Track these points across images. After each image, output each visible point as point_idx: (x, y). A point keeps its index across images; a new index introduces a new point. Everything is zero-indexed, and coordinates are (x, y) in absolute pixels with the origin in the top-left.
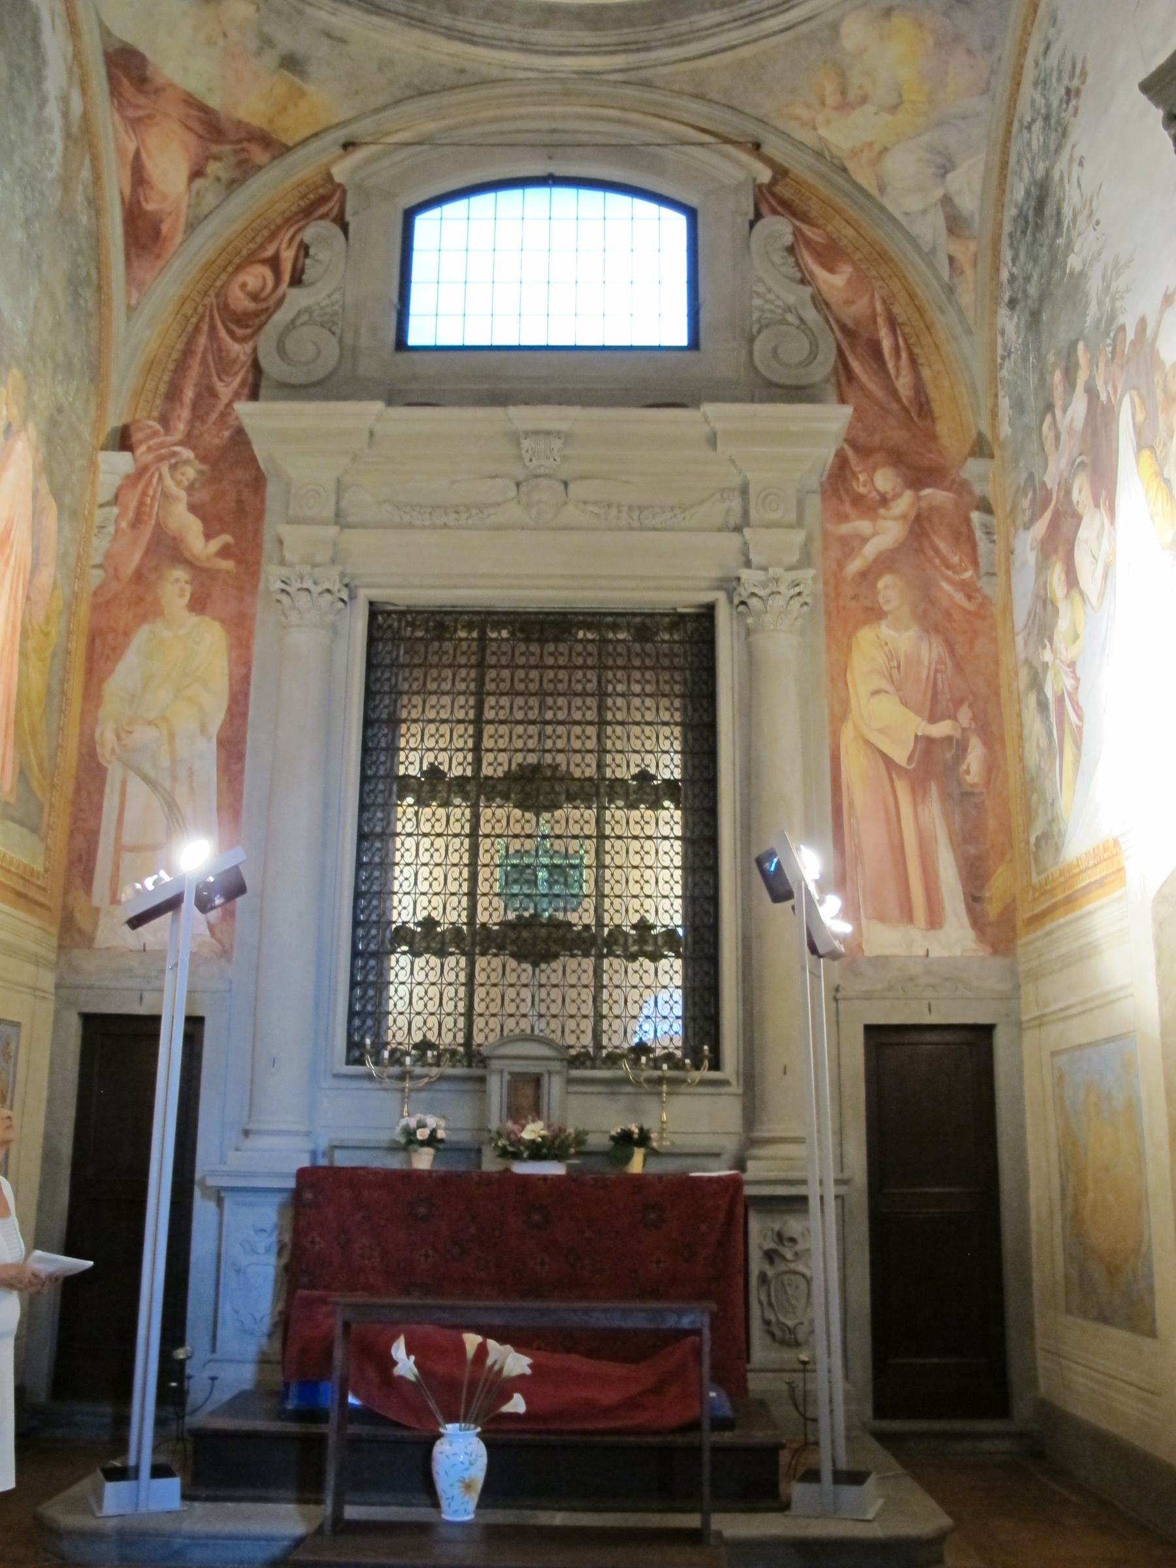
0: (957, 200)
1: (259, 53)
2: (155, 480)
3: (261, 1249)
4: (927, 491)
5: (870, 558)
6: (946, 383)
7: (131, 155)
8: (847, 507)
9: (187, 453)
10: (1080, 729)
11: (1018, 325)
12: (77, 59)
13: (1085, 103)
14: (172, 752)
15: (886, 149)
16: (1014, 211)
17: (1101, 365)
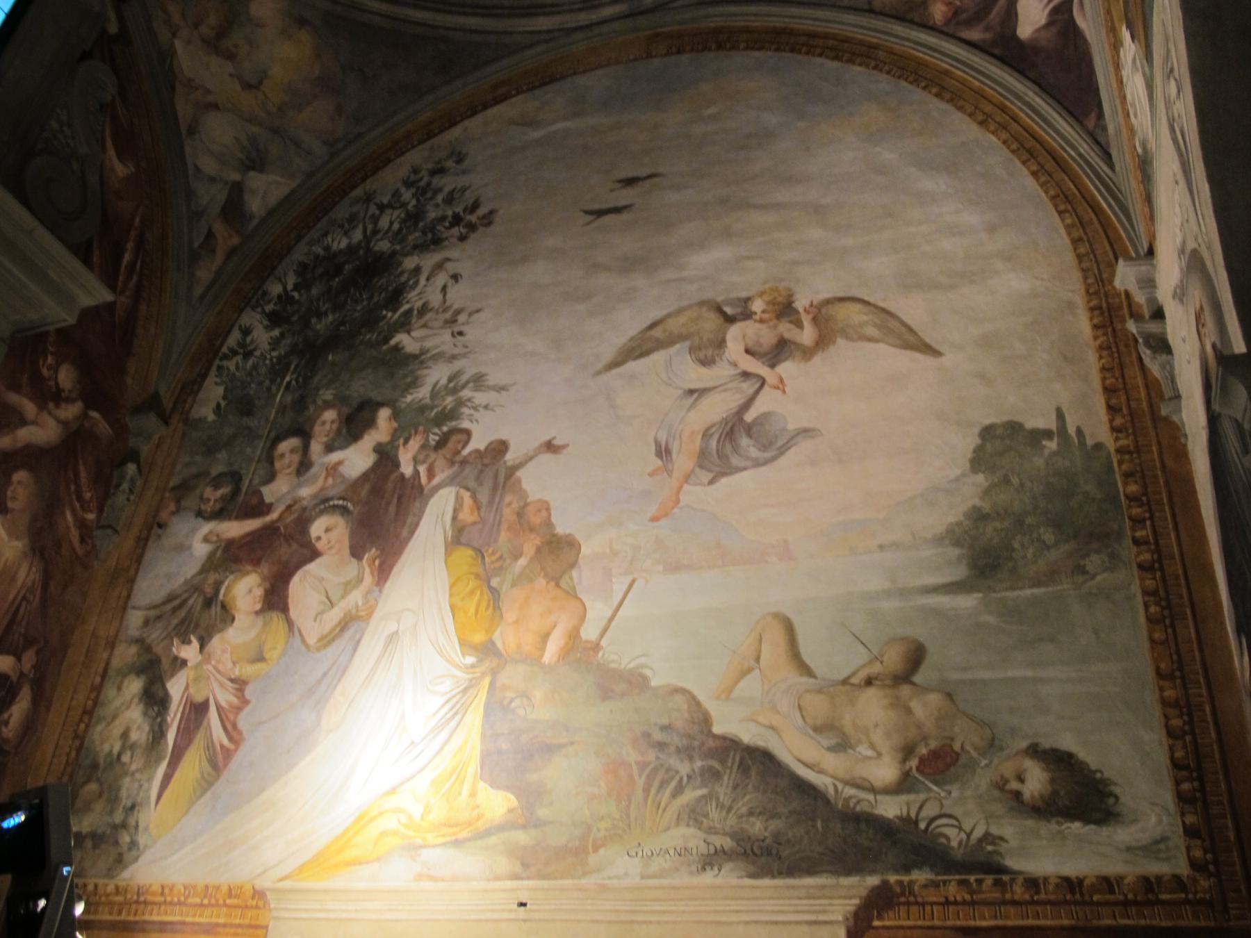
0: (247, 197)
4: (94, 414)
5: (20, 444)
13: (480, 242)
15: (215, 106)
16: (319, 250)
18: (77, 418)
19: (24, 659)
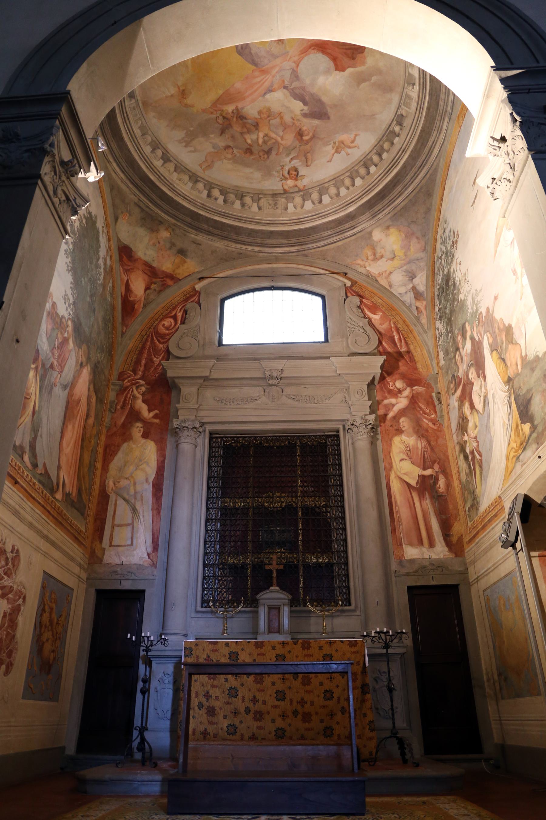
0: (418, 288)
1: (170, 248)
2: (130, 392)
3: (166, 682)
5: (396, 412)
6: (419, 350)
7: (125, 281)
8: (386, 394)
9: (142, 382)
10: (481, 460)
11: (443, 325)
12: (109, 249)
13: (460, 244)
14: (135, 489)
15: (391, 273)
16: (438, 287)
17: (475, 328)
18: (410, 392)
19: (435, 467)
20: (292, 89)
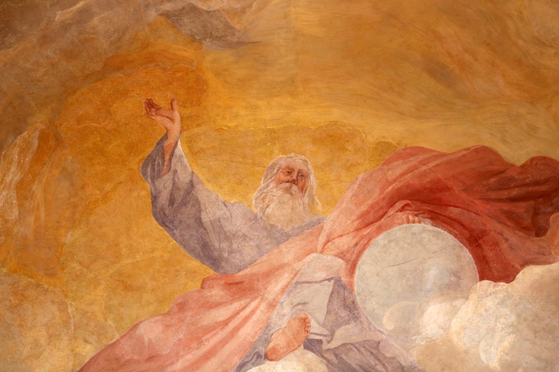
20: (335, 352)
